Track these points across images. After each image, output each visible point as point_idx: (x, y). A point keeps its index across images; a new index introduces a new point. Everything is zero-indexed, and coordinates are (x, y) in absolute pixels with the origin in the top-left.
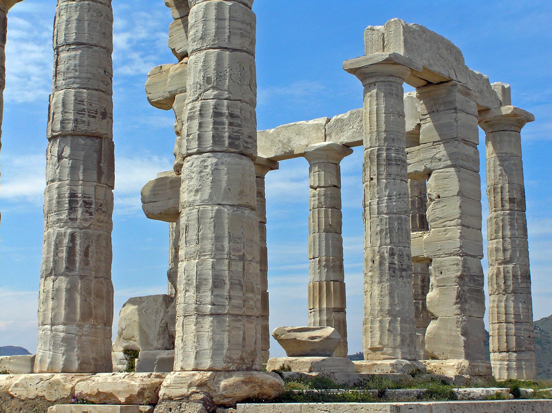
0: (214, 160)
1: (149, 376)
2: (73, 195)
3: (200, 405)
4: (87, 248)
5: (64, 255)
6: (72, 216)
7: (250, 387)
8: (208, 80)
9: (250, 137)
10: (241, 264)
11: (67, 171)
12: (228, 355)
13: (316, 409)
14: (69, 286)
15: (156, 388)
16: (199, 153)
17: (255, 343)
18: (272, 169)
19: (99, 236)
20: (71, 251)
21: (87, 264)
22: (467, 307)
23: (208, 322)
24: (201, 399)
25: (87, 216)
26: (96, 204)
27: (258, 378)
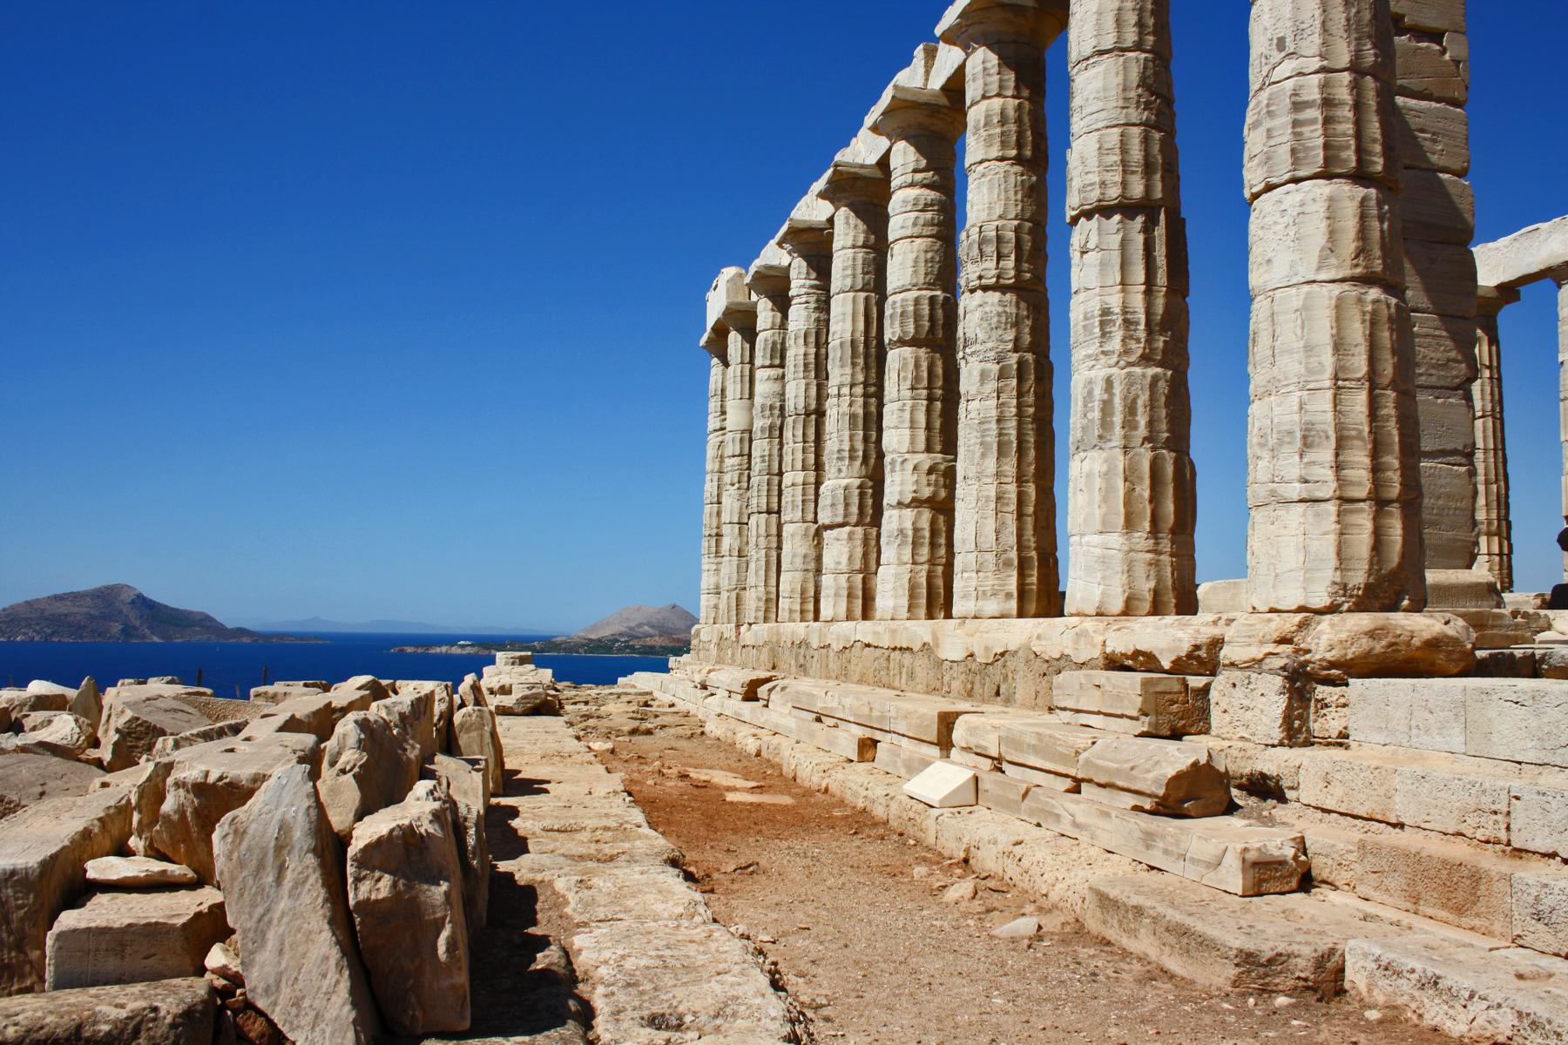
0: (1298, 197)
1: (1215, 623)
2: (1106, 312)
3: (1278, 681)
4: (1134, 401)
5: (1096, 415)
6: (1107, 348)
7: (1384, 643)
10: (1362, 397)
12: (1338, 580)
13: (1495, 697)
14: (1104, 468)
15: (1217, 644)
16: (1270, 188)
19: (1155, 380)
20: (1107, 407)
21: (1134, 427)
24: (1283, 668)
25: (1133, 345)
26: (1148, 323)
27: (1402, 627)
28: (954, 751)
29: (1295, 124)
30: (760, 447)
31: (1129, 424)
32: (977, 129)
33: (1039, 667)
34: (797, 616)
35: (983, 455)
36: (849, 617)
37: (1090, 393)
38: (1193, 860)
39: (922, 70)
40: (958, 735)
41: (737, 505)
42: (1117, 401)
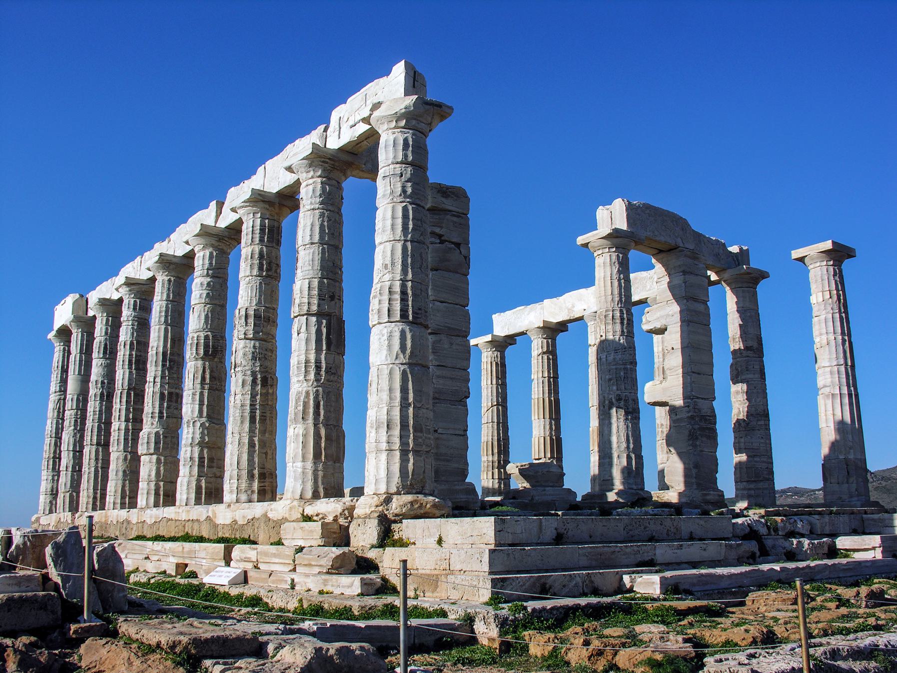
2: (307, 362)
5: (301, 408)
8: (386, 266)
9: (420, 309)
11: (304, 343)
17: (424, 472)
18: (562, 331)
20: (305, 405)
22: (698, 443)
23: (384, 456)
28: (232, 563)
29: (390, 300)
30: (93, 406)
31: (317, 413)
32: (246, 259)
33: (271, 524)
34: (119, 506)
35: (242, 422)
36: (156, 505)
37: (299, 398)
38: (343, 587)
39: (214, 214)
40: (233, 555)
41: (72, 440)
42: (312, 402)
